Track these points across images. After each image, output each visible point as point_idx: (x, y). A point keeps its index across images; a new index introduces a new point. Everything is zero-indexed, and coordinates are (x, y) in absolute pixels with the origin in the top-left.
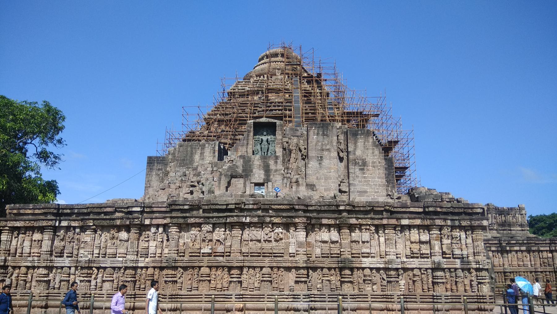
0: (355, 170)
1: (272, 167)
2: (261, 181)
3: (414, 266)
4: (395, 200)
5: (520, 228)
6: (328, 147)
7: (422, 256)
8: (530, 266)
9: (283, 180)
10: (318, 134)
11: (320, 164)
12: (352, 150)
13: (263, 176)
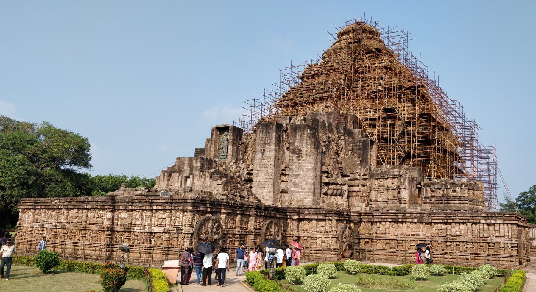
1: (195, 165)
2: (188, 175)
3: (157, 231)
4: (361, 177)
5: (457, 202)
6: (269, 142)
7: (161, 226)
9: (200, 173)
10: (263, 132)
11: (263, 155)
12: (292, 142)
13: (189, 171)
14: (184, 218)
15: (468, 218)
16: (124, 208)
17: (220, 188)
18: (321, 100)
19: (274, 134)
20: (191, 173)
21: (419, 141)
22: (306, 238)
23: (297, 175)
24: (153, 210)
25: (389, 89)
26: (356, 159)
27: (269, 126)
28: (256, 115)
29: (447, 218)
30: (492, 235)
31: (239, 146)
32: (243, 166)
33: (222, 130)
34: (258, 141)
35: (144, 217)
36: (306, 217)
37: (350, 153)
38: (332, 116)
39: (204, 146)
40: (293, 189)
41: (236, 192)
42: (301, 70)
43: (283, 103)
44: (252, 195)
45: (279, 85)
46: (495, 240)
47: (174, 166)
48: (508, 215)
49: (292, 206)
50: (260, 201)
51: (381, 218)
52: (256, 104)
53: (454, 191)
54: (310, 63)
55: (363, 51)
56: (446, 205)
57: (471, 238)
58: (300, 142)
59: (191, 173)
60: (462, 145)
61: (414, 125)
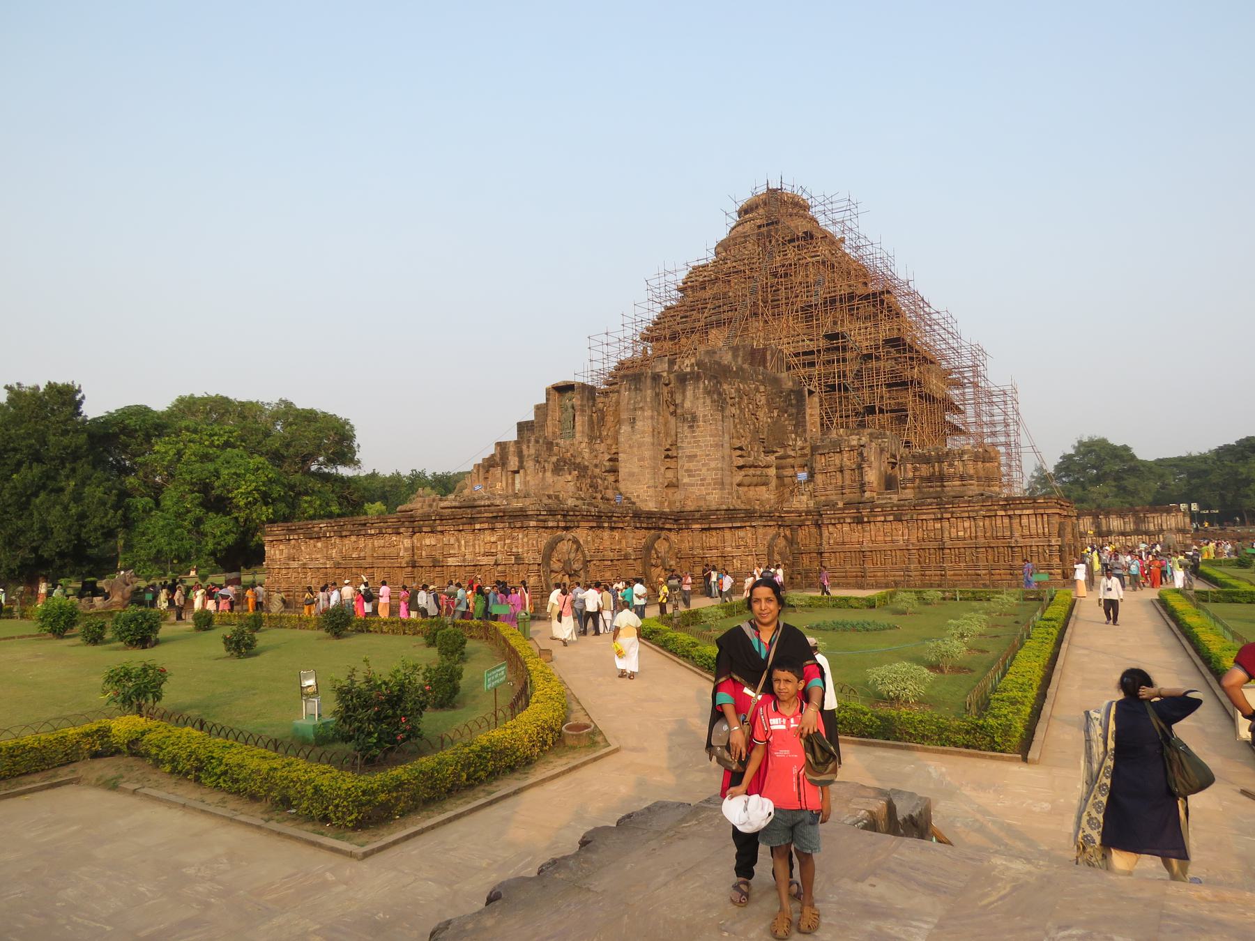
1: (525, 452)
2: (516, 469)
6: (641, 405)
7: (492, 554)
8: (901, 543)
13: (517, 463)
14: (525, 540)
15: (976, 508)
16: (428, 529)
17: (571, 487)
18: (719, 324)
19: (649, 392)
20: (521, 466)
21: (889, 385)
22: (715, 559)
23: (692, 458)
24: (474, 530)
25: (833, 301)
26: (787, 423)
27: (640, 379)
28: (611, 359)
29: (942, 510)
30: (1017, 534)
31: (591, 416)
32: (601, 447)
33: (563, 389)
34: (623, 403)
35: (463, 542)
36: (712, 526)
37: (776, 415)
38: (741, 353)
39: (531, 417)
40: (686, 480)
41: (596, 492)
42: (683, 275)
43: (654, 334)
44: (621, 494)
45: (645, 305)
46: (1021, 542)
47: (493, 456)
48: (1042, 501)
49: (688, 509)
50: (634, 503)
51: (835, 519)
52: (611, 340)
53: (951, 465)
54: (696, 264)
55: (783, 238)
56: (939, 489)
57: (983, 540)
59: (521, 466)
60: (959, 384)
61: (878, 358)
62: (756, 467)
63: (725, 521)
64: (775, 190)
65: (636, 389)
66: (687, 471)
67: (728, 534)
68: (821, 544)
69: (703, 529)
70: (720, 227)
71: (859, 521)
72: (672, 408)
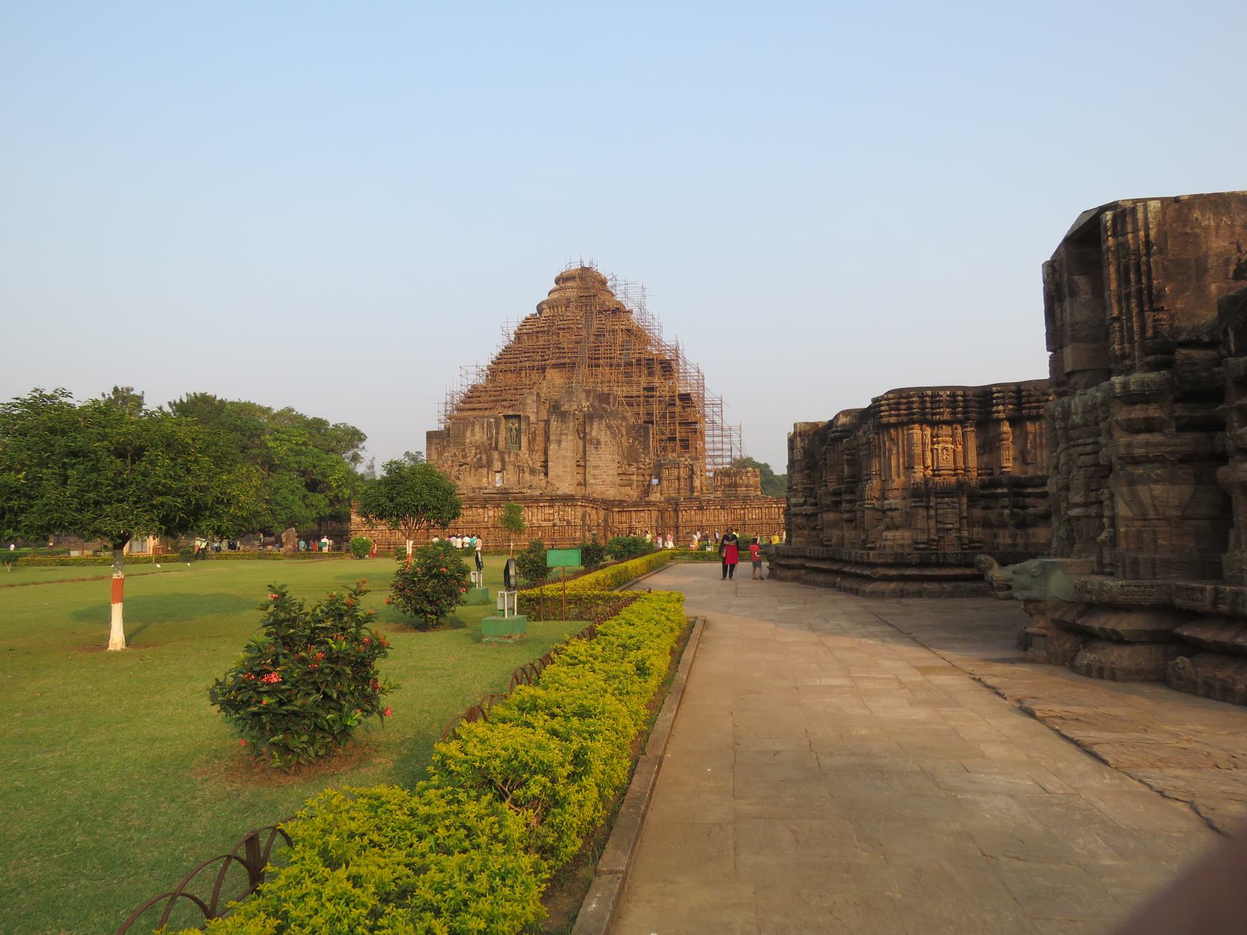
0: (591, 449)
1: (507, 459)
7: (549, 520)
10: (557, 421)
23: (596, 467)
32: (536, 457)
38: (592, 395)
40: (591, 481)
53: (741, 479)
58: (598, 433)
62: (626, 474)
63: (632, 507)
64: (587, 269)
65: (562, 421)
66: (594, 475)
67: (634, 515)
68: (678, 522)
69: (619, 511)
70: (540, 289)
71: (701, 508)
72: (582, 435)
